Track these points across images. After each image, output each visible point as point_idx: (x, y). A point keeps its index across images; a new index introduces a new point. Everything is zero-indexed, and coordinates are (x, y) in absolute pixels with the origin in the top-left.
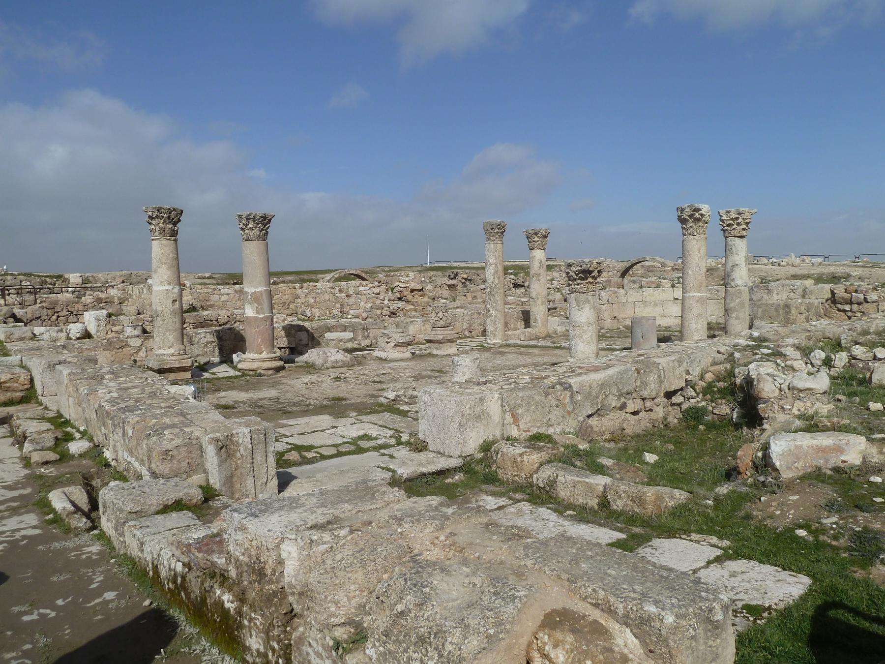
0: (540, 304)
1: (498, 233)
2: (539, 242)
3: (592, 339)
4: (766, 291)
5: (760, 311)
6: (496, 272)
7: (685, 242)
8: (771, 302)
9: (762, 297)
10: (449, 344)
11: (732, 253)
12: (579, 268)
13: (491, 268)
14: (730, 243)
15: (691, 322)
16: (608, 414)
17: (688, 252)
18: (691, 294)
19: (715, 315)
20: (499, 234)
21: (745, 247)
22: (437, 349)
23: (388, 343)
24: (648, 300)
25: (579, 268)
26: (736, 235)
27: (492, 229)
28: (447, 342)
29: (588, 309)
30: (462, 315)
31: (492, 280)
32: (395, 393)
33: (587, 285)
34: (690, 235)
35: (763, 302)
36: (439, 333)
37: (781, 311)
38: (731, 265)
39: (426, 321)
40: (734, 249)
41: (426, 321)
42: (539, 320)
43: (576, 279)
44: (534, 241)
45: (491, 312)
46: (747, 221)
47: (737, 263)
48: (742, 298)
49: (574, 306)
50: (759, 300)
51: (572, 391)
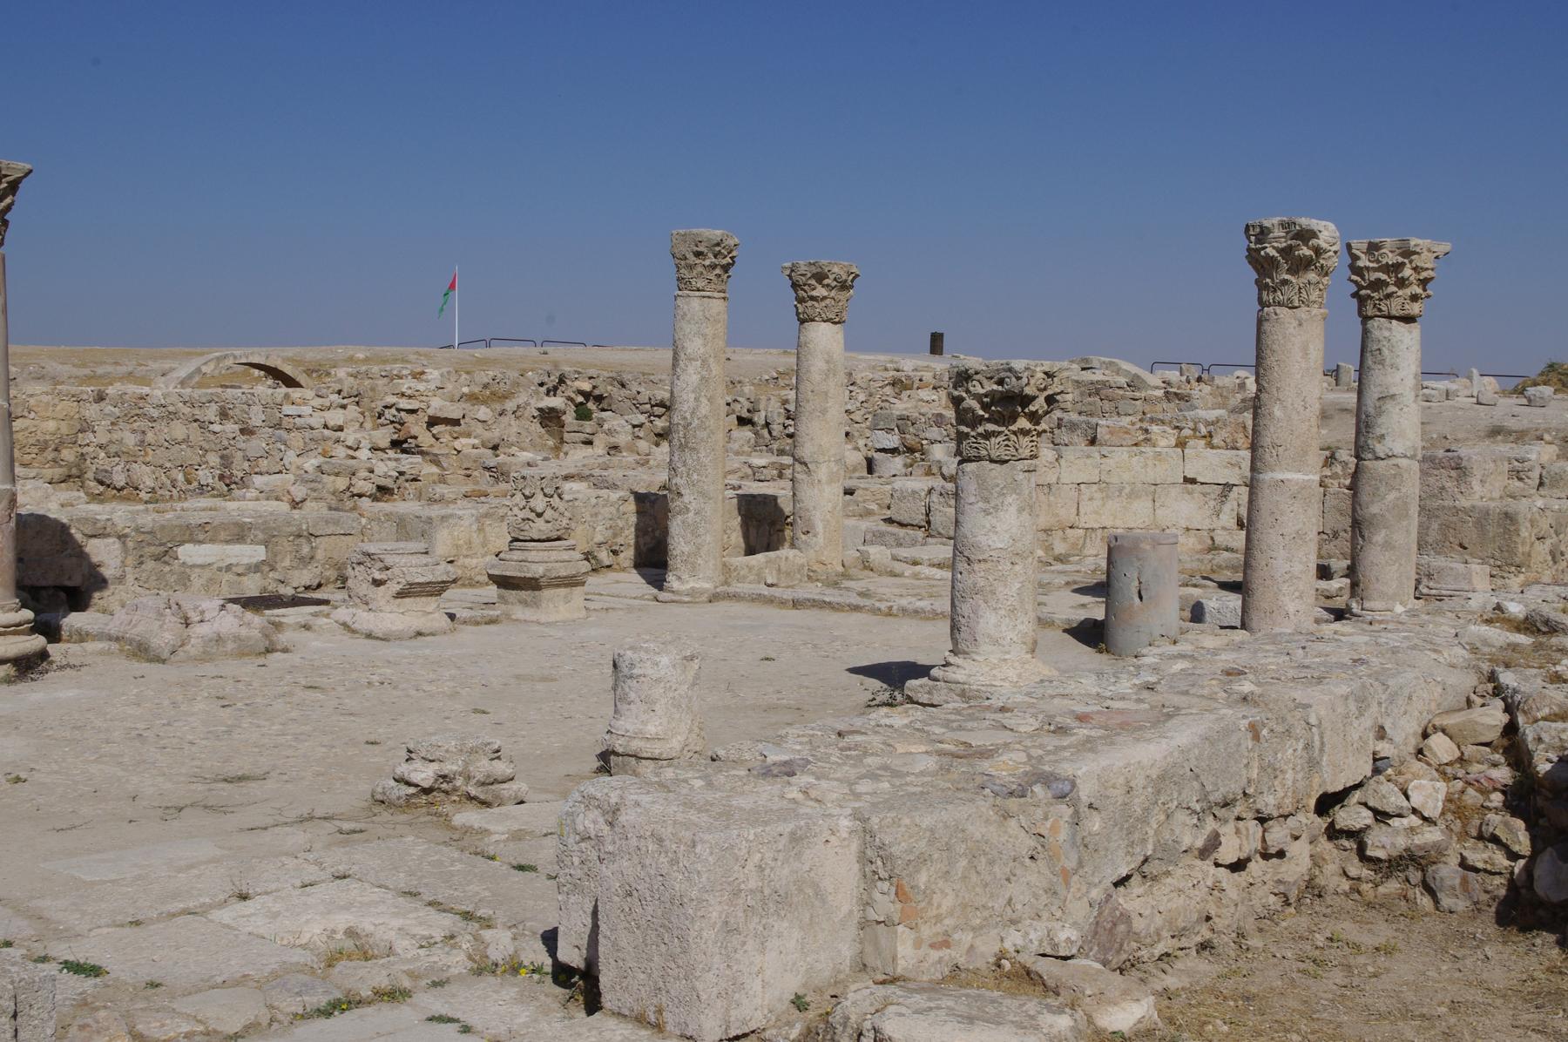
0: (824, 478)
1: (713, 267)
2: (828, 301)
3: (1022, 602)
4: (1453, 473)
5: (1435, 526)
6: (704, 380)
7: (1266, 326)
8: (1464, 502)
9: (1443, 488)
10: (562, 591)
11: (1382, 362)
12: (995, 387)
13: (691, 370)
14: (1376, 333)
15: (1274, 554)
16: (1168, 873)
18: (1280, 476)
20: (718, 271)
21: (1416, 347)
22: (524, 603)
23: (377, 583)
24: (1114, 479)
25: (995, 387)
26: (1394, 313)
27: (698, 254)
28: (558, 586)
29: (1013, 509)
30: (594, 501)
31: (692, 403)
32: (435, 766)
33: (1013, 437)
34: (1280, 304)
35: (1446, 503)
36: (532, 556)
37: (1492, 530)
38: (1376, 396)
39: (487, 515)
40: (1386, 352)
41: (487, 515)
42: (820, 527)
43: (981, 420)
44: (813, 298)
45: (686, 499)
46: (1424, 275)
47: (1393, 390)
48: (1404, 490)
49: (972, 499)
51: (1074, 805)
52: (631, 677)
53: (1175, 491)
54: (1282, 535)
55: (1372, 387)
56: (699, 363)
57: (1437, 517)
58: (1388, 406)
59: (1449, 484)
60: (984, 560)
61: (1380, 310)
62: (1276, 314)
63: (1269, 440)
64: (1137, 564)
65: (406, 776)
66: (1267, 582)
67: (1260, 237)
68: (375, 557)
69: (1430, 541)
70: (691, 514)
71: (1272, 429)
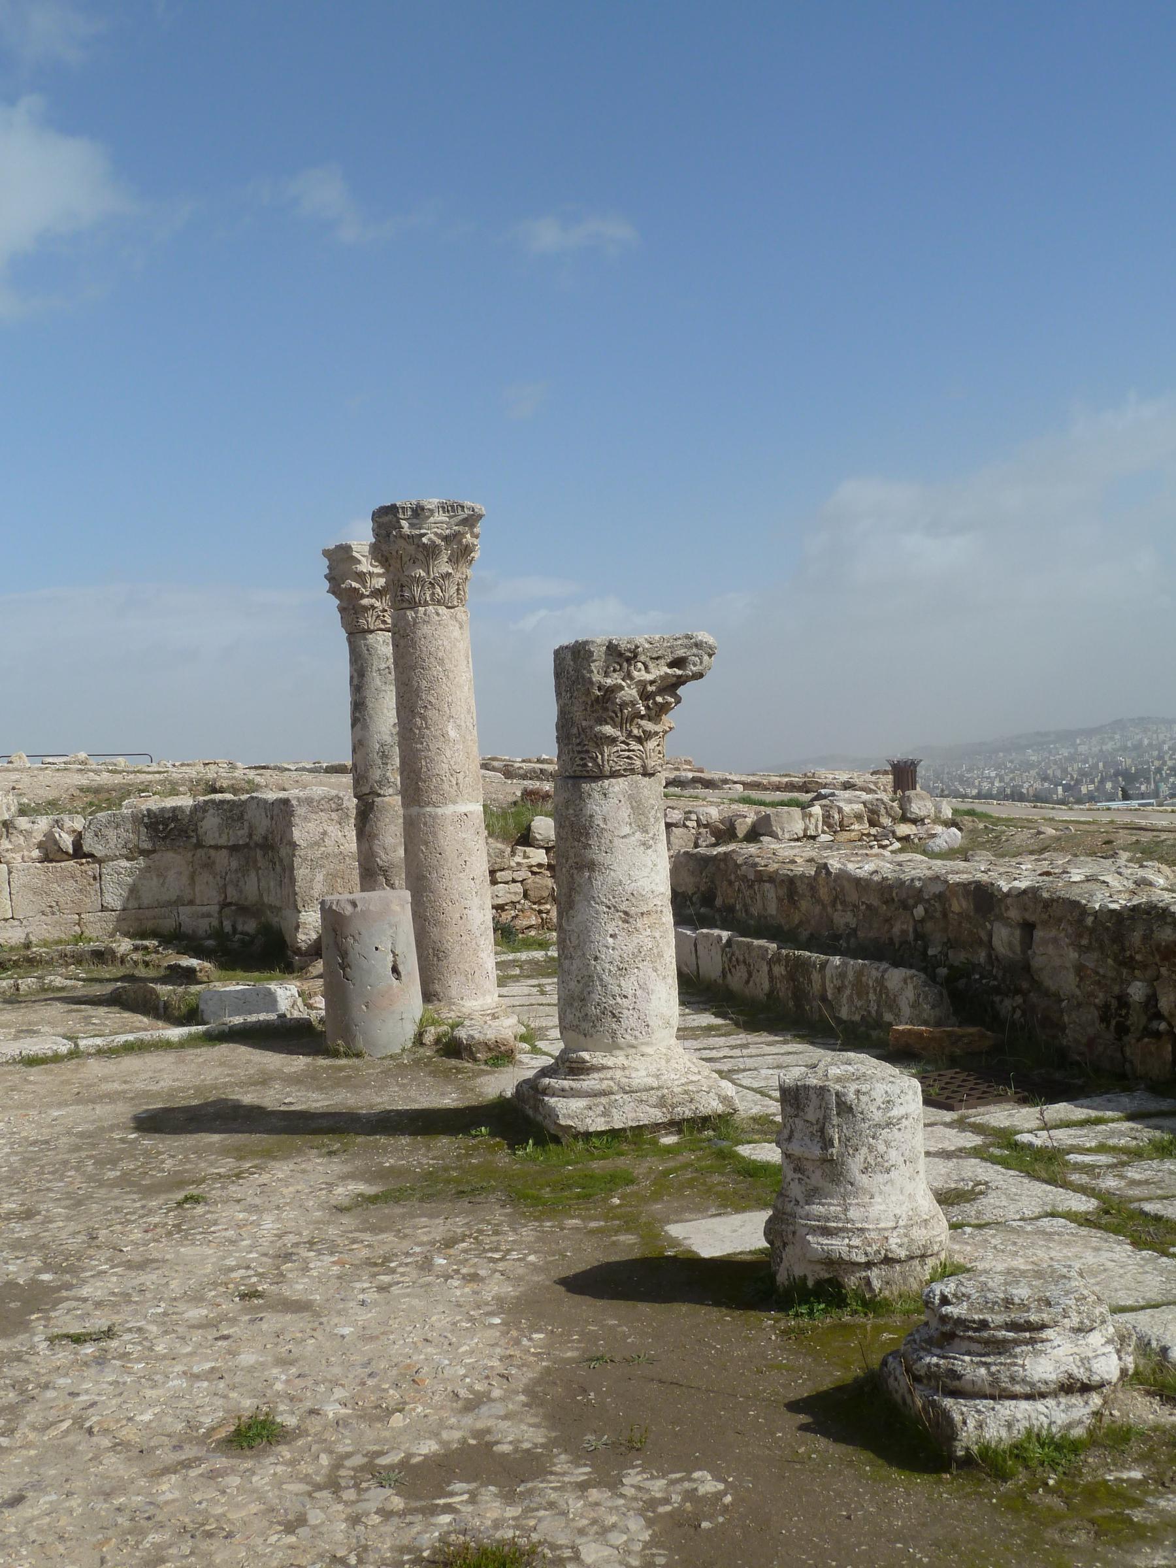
4: (334, 815)
5: (320, 877)
9: (325, 833)
15: (468, 903)
17: (441, 662)
35: (330, 850)
49: (626, 830)
50: (317, 844)
52: (889, 1124)
54: (473, 879)
55: (385, 711)
57: (322, 866)
59: (331, 828)
60: (649, 913)
61: (384, 622)
62: (438, 614)
63: (445, 766)
64: (390, 932)
65: (1081, 1374)
66: (464, 938)
67: (415, 521)
69: (316, 895)
71: (448, 753)
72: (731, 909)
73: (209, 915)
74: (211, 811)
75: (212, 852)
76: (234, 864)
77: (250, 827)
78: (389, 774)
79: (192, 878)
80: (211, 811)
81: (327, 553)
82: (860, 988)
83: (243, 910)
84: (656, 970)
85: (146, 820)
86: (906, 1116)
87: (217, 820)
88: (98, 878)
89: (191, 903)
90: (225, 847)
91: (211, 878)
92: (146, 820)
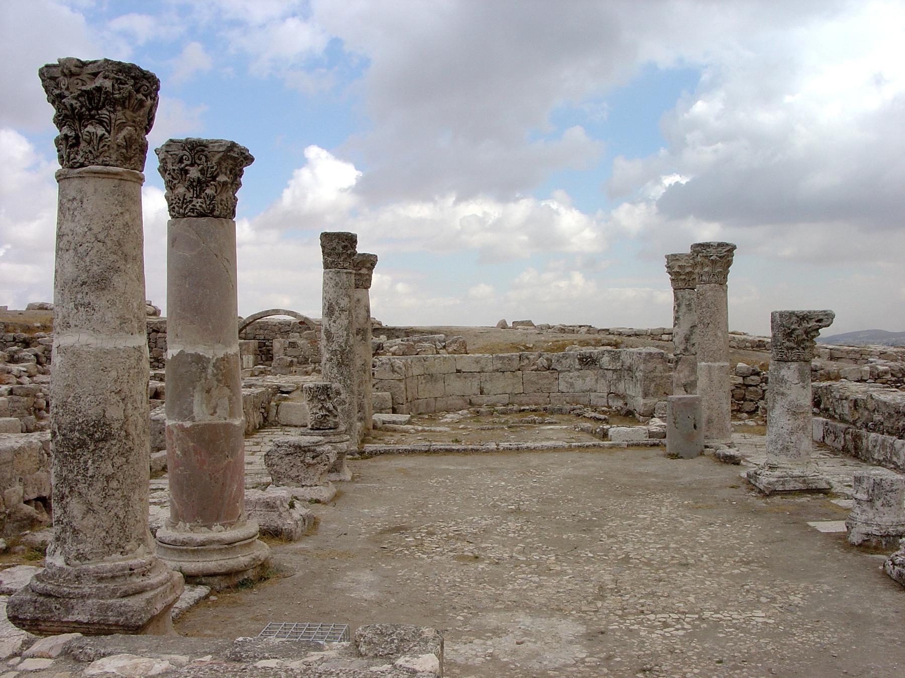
5: (653, 385)
9: (656, 367)
13: (343, 317)
19: (508, 391)
35: (657, 374)
53: (453, 377)
56: (347, 312)
58: (695, 330)
68: (306, 449)
70: (347, 405)
72: (827, 410)
73: (603, 397)
74: (606, 355)
75: (606, 371)
76: (615, 377)
77: (623, 362)
78: (688, 347)
79: (597, 380)
80: (606, 355)
81: (667, 257)
82: (883, 446)
83: (618, 396)
84: (804, 433)
85: (579, 356)
86: (898, 489)
87: (608, 358)
88: (557, 379)
89: (595, 391)
90: (611, 370)
91: (604, 382)
92: (579, 356)
